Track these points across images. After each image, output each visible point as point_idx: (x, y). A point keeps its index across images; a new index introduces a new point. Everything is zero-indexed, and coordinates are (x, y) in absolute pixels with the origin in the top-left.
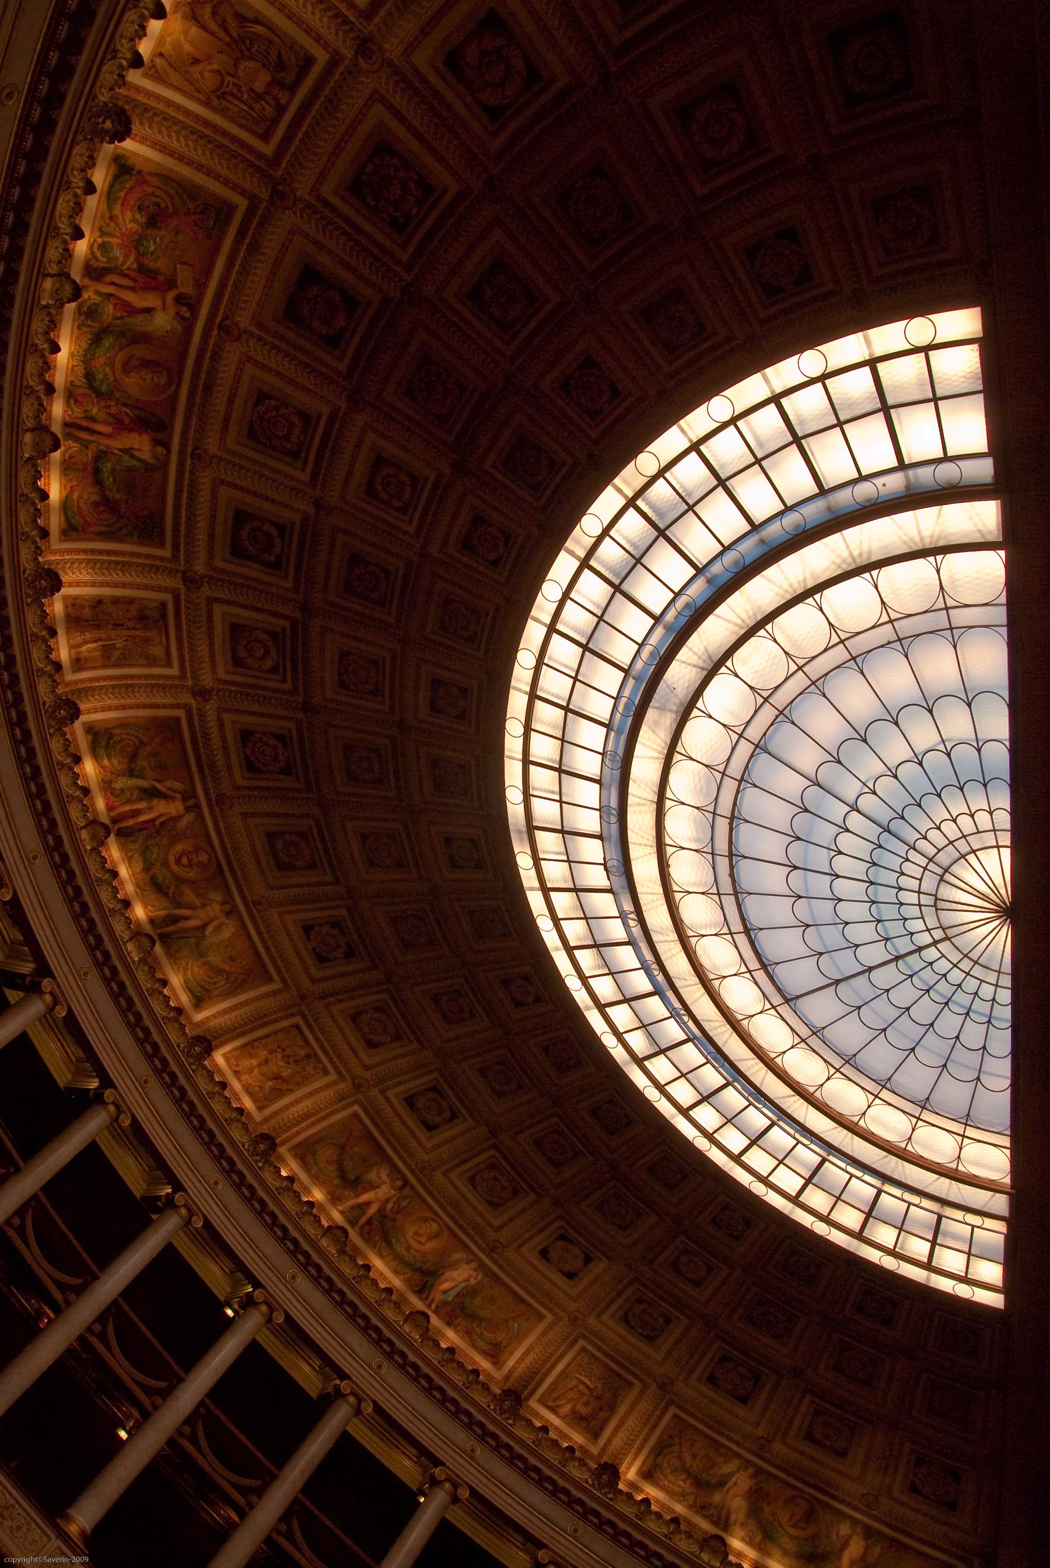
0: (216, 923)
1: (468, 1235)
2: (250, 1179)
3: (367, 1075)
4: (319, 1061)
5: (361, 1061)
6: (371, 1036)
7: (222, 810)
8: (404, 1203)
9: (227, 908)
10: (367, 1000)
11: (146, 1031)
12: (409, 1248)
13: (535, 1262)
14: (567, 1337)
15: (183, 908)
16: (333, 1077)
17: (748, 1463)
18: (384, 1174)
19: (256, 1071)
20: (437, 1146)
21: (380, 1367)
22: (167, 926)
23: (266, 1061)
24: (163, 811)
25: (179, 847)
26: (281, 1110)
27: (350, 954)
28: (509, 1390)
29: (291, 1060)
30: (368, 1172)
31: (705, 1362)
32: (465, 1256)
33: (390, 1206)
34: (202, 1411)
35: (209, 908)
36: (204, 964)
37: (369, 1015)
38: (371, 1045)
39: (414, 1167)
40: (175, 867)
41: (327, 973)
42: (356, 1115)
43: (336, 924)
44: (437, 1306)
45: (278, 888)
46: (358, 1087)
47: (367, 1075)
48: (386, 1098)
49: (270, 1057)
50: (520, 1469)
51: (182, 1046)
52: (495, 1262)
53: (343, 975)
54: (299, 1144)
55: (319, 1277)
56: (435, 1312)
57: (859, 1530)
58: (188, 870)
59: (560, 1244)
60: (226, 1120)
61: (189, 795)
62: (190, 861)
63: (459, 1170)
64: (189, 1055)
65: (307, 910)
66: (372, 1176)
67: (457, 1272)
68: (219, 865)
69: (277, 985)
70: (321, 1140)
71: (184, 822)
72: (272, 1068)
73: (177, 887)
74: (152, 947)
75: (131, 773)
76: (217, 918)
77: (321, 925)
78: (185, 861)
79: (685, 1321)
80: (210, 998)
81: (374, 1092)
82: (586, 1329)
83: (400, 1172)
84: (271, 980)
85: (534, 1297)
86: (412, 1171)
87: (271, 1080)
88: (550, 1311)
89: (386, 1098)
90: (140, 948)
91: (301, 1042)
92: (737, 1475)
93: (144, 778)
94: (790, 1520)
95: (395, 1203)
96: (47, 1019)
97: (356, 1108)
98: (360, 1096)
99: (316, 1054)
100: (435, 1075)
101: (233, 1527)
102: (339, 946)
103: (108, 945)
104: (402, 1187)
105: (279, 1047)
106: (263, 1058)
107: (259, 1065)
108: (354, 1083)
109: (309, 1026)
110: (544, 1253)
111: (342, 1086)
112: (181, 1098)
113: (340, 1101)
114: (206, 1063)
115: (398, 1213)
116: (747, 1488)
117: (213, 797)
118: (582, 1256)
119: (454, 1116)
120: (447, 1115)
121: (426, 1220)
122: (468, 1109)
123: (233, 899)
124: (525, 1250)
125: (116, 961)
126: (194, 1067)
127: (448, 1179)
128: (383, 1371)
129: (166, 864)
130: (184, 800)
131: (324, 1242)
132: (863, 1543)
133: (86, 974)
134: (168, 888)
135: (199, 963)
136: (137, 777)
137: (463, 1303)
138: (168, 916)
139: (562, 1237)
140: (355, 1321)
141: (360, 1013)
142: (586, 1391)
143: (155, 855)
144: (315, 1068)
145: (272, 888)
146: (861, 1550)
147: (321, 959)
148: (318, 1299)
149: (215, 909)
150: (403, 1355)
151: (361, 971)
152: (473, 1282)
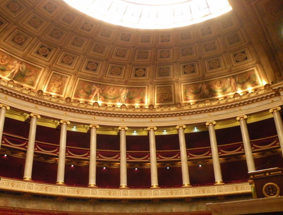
1: (119, 84)
2: (71, 108)
3: (75, 71)
4: (64, 76)
5: (71, 69)
8: (103, 89)
10: (62, 56)
11: (27, 98)
12: (111, 96)
13: (135, 79)
14: (153, 88)
15: (12, 70)
16: (69, 77)
17: (203, 83)
18: (95, 86)
19: (55, 88)
21: (123, 120)
22: (13, 76)
23: (55, 85)
27: (50, 50)
28: (150, 105)
29: (59, 81)
31: (181, 71)
32: (122, 89)
33: (101, 91)
35: (17, 66)
36: (26, 77)
38: (70, 64)
40: (3, 64)
41: (50, 57)
42: (80, 80)
43: (42, 47)
44: (125, 102)
45: (24, 50)
46: (75, 75)
47: (75, 71)
48: (82, 72)
49: (55, 83)
50: (162, 117)
51: (37, 95)
52: (128, 85)
53: (53, 55)
55: (99, 114)
56: (125, 103)
57: (232, 78)
58: (5, 62)
59: (137, 71)
60: (57, 101)
62: (4, 60)
63: (107, 73)
64: (39, 96)
66: (93, 89)
67: (123, 93)
68: (10, 55)
69: (43, 69)
70: (78, 90)
72: (57, 85)
74: (13, 82)
76: (20, 66)
77: (39, 49)
78: (3, 61)
79: (172, 66)
81: (79, 73)
82: (155, 83)
83: (97, 83)
84: (41, 69)
85: (141, 85)
86: (99, 81)
88: (145, 85)
89: (82, 72)
90: (11, 84)
91: (57, 76)
92: (202, 86)
94: (218, 86)
96: (7, 111)
97: (79, 79)
98: (77, 76)
99: (63, 76)
100: (87, 59)
101: (119, 165)
102: (46, 50)
103: (5, 89)
104: (100, 86)
105: (55, 80)
106: (54, 85)
107: (54, 87)
109: (56, 71)
110: (136, 75)
112: (46, 105)
113: (75, 80)
114: (44, 94)
115: (103, 91)
116: (206, 87)
118: (143, 70)
119: (97, 64)
120: (96, 65)
121: (109, 88)
122: (99, 61)
123: (19, 60)
124: (132, 78)
125: (9, 91)
126: (42, 97)
127: (107, 77)
128: (124, 120)
132: (234, 79)
133: (6, 98)
134: (5, 69)
135: (25, 78)
137: (129, 97)
138: (11, 74)
139: (136, 70)
140: (112, 116)
141: (63, 60)
142: (164, 94)
145: (23, 51)
146: (234, 81)
147: (46, 56)
148: (102, 118)
150: (125, 115)
151: (55, 51)
152: (127, 92)
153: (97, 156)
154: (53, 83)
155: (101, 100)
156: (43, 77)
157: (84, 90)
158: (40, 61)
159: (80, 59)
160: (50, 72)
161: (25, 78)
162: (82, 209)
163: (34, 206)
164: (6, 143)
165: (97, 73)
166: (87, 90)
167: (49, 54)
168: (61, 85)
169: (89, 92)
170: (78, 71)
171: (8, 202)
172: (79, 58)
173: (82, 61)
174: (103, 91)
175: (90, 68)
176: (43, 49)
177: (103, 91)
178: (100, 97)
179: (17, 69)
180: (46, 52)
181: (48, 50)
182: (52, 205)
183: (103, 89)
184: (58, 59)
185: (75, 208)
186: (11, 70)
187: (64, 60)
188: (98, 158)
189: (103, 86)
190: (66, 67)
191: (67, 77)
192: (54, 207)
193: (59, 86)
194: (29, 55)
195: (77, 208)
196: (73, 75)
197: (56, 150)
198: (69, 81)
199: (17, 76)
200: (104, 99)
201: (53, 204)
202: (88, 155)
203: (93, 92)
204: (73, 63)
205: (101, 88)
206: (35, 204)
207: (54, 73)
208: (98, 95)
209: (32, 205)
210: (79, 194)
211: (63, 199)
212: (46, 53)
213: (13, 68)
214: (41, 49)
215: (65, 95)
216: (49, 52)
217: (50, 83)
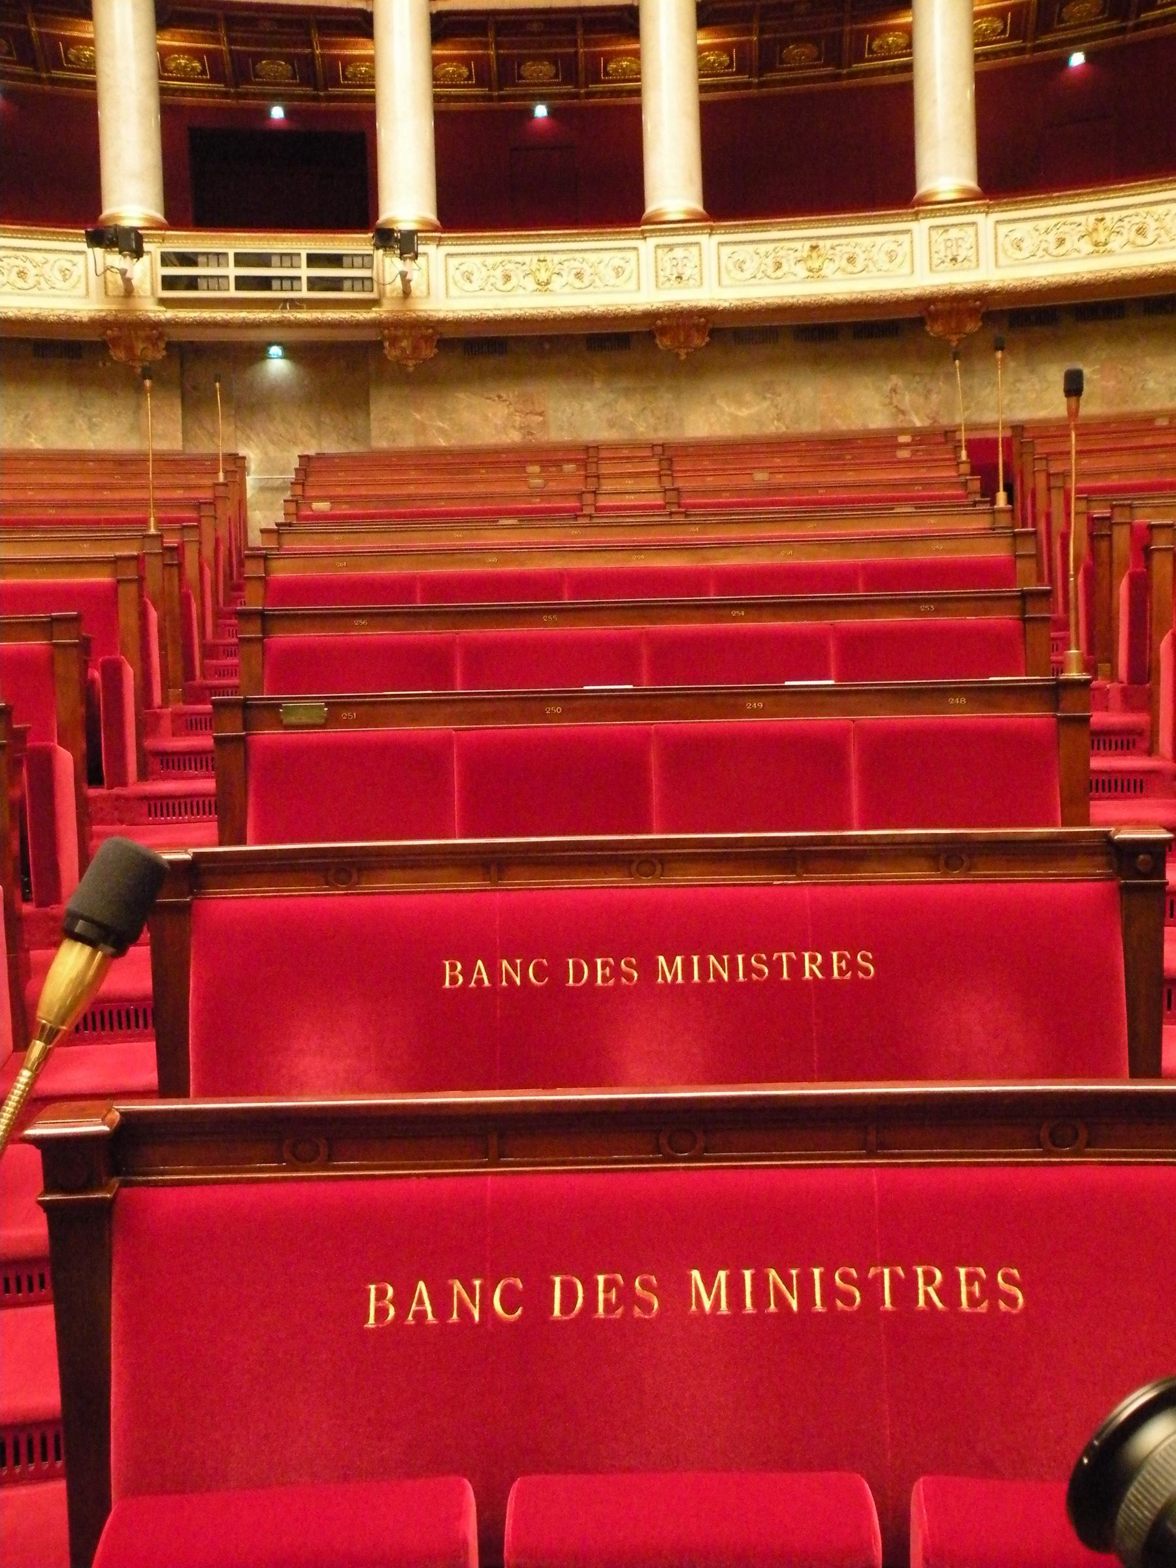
163: (744, 413)
171: (541, 414)
192: (907, 399)
201: (896, 380)
206: (748, 397)
209: (728, 408)
210: (1111, 252)
211: (972, 327)
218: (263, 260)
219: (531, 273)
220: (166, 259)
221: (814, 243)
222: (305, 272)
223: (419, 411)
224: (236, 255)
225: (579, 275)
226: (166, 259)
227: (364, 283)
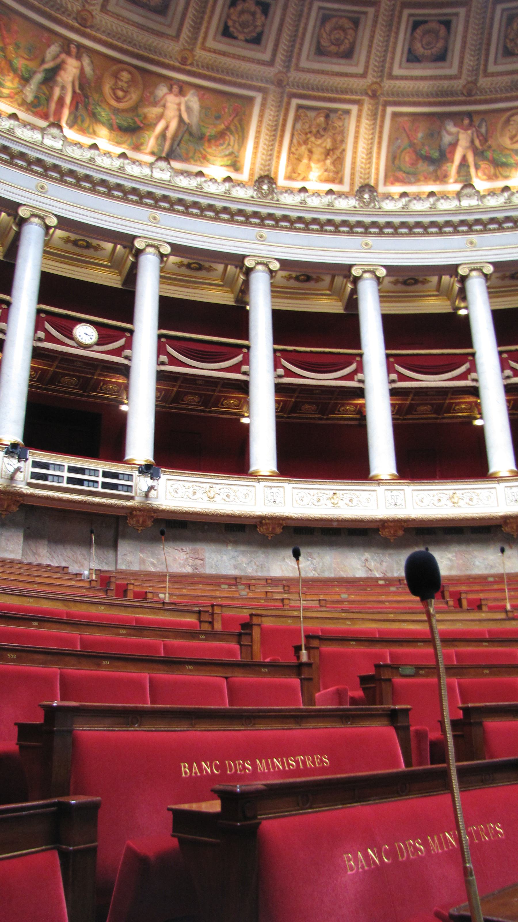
0: (183, 108)
3: (370, 79)
4: (335, 111)
6: (342, 48)
7: (91, 27)
8: (483, 130)
9: (175, 89)
16: (354, 109)
18: (451, 128)
19: (313, 165)
20: (461, 67)
22: (164, 145)
23: (310, 151)
24: (70, 79)
25: (107, 89)
26: (353, 168)
29: (322, 133)
30: (441, 139)
33: (477, 143)
34: (505, 356)
36: (209, 141)
37: (325, 36)
39: (463, 98)
42: (395, 115)
46: (374, 96)
47: (370, 79)
48: (397, 78)
49: (309, 146)
54: (386, 176)
61: (67, 46)
62: (122, 89)
65: (211, 18)
66: (447, 139)
70: (394, 158)
71: (88, 70)
72: (318, 152)
73: (138, 116)
75: (25, 80)
76: (179, 105)
77: (228, 16)
78: (120, 94)
80: (236, 157)
84: (251, 100)
87: (326, 159)
89: (397, 78)
91: (312, 114)
93: (35, 73)
95: (478, 137)
98: (382, 99)
104: (471, 121)
105: (306, 134)
107: (310, 159)
108: (369, 96)
111: (366, 108)
113: (375, 119)
115: (486, 140)
117: (76, 25)
119: (447, 24)
121: (508, 121)
129: (117, 111)
130: (69, 53)
131: (465, 203)
134: (135, 122)
136: (31, 77)
138: (157, 138)
143: (103, 114)
144: (340, 118)
145: (177, 37)
149: (172, 100)
153: (503, 369)
154: (303, 148)
155: (485, 177)
156: (264, 130)
157: (415, 152)
158: (245, 66)
159: (380, 20)
160: (284, 104)
161: (206, 144)
162: (477, 563)
164: (173, 361)
165: (451, 66)
166: (427, 148)
167: (266, 31)
168: (334, 149)
169: (436, 155)
170: (381, 77)
171: (202, 560)
172: (376, 17)
173: (389, 26)
174: (485, 140)
175: (421, 50)
176: (242, 12)
177: (485, 140)
178: (477, 168)
179: (174, 117)
180: (254, 20)
181: (258, 11)
182: (366, 560)
183: (483, 130)
184: (302, 44)
185: (451, 560)
186: (151, 126)
187: (325, 43)
188: (508, 377)
189: (483, 120)
190: (336, 68)
191: (348, 112)
192: (372, 564)
193: (328, 153)
194: (199, 53)
195: (461, 562)
196: (366, 99)
197: (353, 367)
198: (358, 127)
199: (178, 145)
200: (492, 171)
201: (367, 555)
202: (469, 371)
203: (450, 152)
204: (357, 49)
205: (477, 131)
207: (299, 107)
208: (471, 159)
210: (459, 506)
212: (256, 27)
213: (161, 116)
214: (234, 13)
215: (352, 184)
216: (263, 18)
217: (293, 149)
218: (81, 471)
219: (206, 492)
220: (36, 464)
221: (334, 491)
222: (101, 479)
223: (142, 552)
224: (69, 467)
225: (228, 496)
226: (36, 464)
227: (129, 488)
